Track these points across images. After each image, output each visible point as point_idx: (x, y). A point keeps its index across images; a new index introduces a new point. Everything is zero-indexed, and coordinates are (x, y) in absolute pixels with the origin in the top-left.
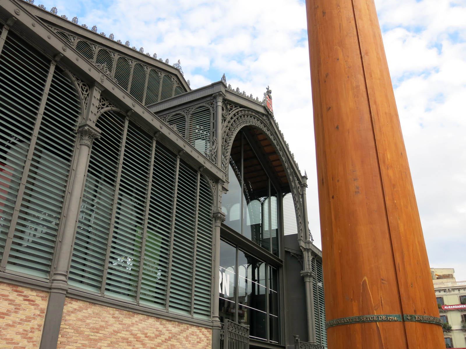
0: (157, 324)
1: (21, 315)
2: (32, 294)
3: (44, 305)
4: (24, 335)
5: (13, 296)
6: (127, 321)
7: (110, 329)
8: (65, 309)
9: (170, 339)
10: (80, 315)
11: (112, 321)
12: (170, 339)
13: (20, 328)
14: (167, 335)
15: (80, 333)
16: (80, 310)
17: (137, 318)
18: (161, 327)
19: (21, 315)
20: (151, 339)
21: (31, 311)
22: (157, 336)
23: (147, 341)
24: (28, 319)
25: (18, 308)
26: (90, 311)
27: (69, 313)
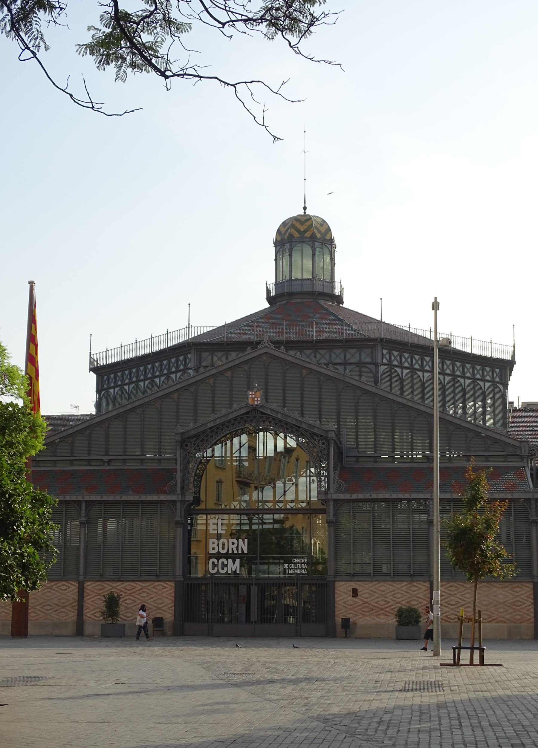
0: (133, 584)
1: (70, 589)
2: (73, 583)
3: (77, 585)
4: (72, 594)
5: (67, 584)
6: (114, 585)
7: (107, 589)
8: (85, 585)
9: (141, 589)
10: (92, 586)
11: (107, 586)
12: (141, 589)
13: (71, 593)
14: (139, 588)
15: (93, 592)
16: (92, 584)
17: (120, 583)
18: (135, 585)
19: (70, 589)
20: (129, 590)
21: (73, 587)
22: (132, 589)
23: (126, 591)
24: (73, 590)
25: (69, 587)
26: (96, 584)
27: (87, 586)
